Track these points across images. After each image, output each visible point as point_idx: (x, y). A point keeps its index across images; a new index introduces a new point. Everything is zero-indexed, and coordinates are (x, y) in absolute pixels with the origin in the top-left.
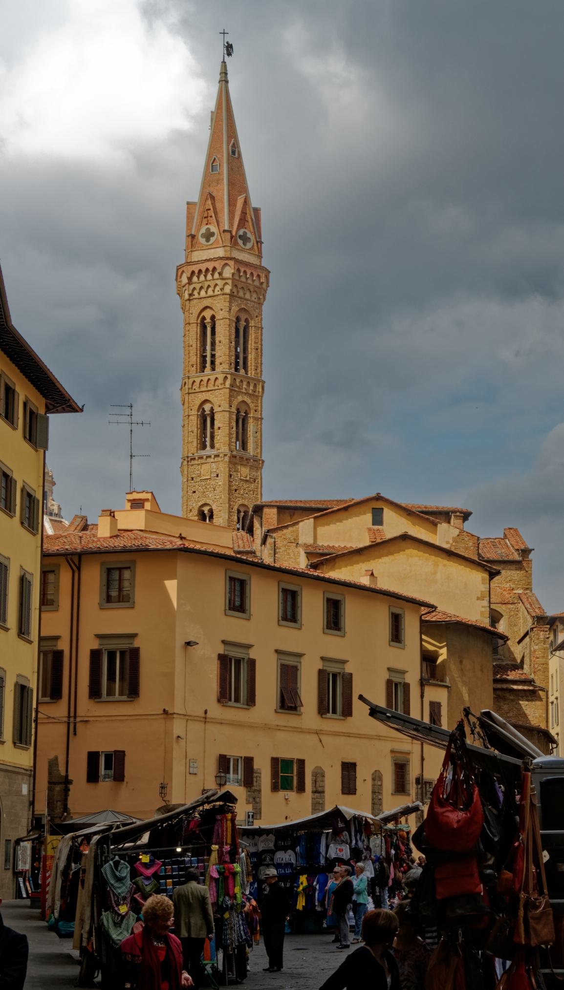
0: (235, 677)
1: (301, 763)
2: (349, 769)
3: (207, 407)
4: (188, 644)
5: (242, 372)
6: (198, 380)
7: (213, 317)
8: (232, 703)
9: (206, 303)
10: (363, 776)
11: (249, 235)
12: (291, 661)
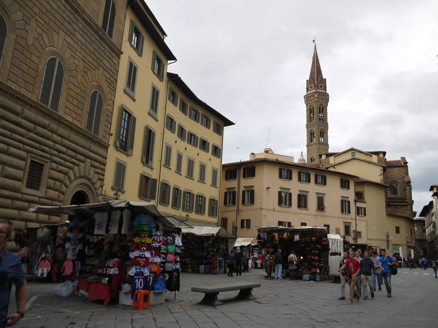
0: (284, 199)
3: (312, 131)
4: (268, 188)
7: (313, 108)
9: (311, 104)
11: (322, 85)
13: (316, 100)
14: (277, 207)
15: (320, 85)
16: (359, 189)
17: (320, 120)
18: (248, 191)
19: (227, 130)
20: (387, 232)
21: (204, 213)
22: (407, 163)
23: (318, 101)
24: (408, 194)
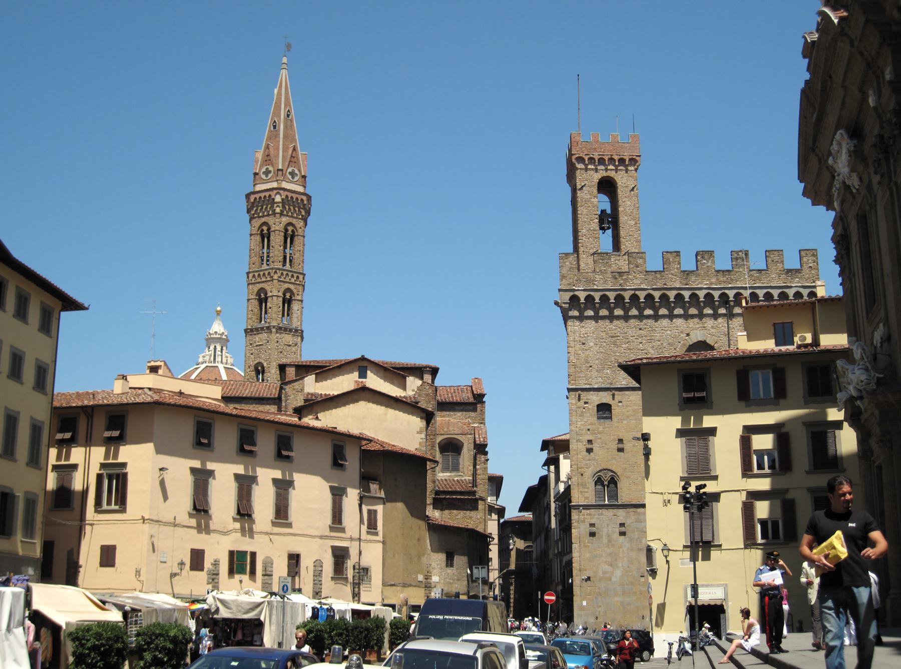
1: (253, 555)
2: (294, 559)
5: (288, 266)
9: (263, 220)
10: (306, 563)
11: (297, 172)
13: (278, 210)
15: (290, 170)
23: (281, 214)
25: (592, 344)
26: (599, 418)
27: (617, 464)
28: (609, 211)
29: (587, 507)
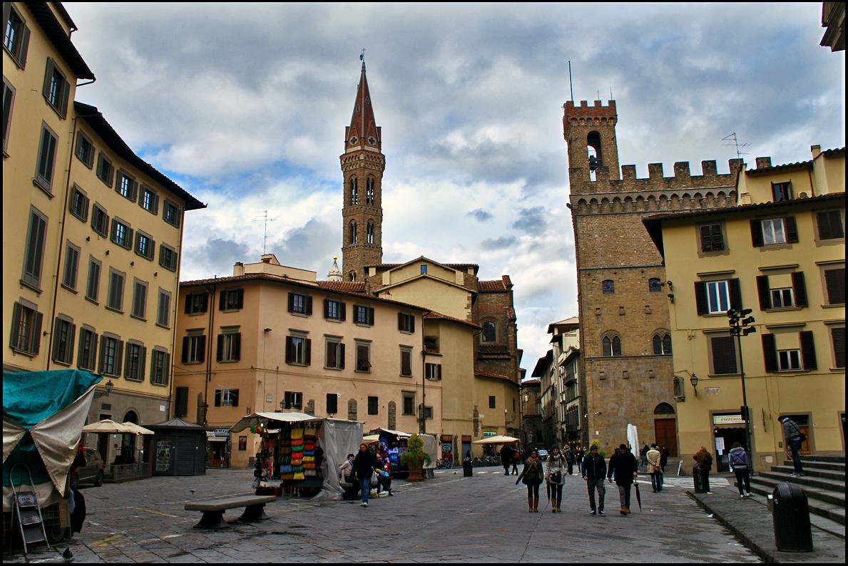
0: (297, 350)
6: (348, 210)
8: (296, 363)
10: (383, 405)
11: (374, 139)
12: (406, 350)
13: (362, 165)
14: (284, 367)
15: (370, 138)
16: (432, 333)
17: (368, 202)
18: (229, 336)
19: (190, 216)
20: (476, 407)
21: (143, 378)
22: (512, 286)
23: (364, 168)
24: (511, 339)
25: (596, 236)
26: (604, 292)
27: (620, 327)
28: (595, 157)
29: (598, 359)
